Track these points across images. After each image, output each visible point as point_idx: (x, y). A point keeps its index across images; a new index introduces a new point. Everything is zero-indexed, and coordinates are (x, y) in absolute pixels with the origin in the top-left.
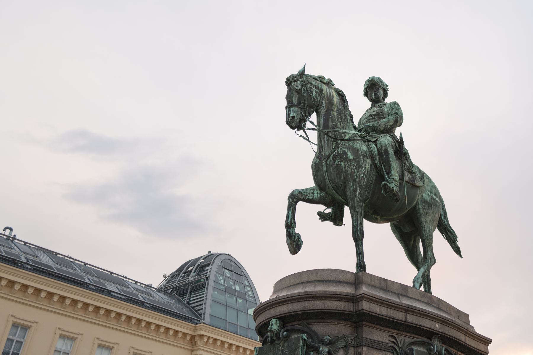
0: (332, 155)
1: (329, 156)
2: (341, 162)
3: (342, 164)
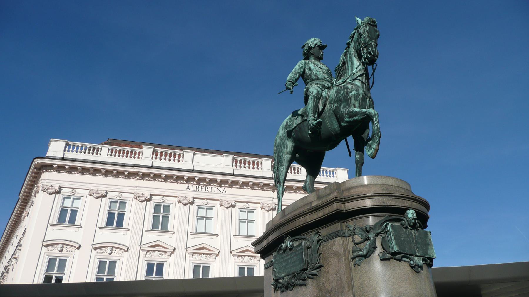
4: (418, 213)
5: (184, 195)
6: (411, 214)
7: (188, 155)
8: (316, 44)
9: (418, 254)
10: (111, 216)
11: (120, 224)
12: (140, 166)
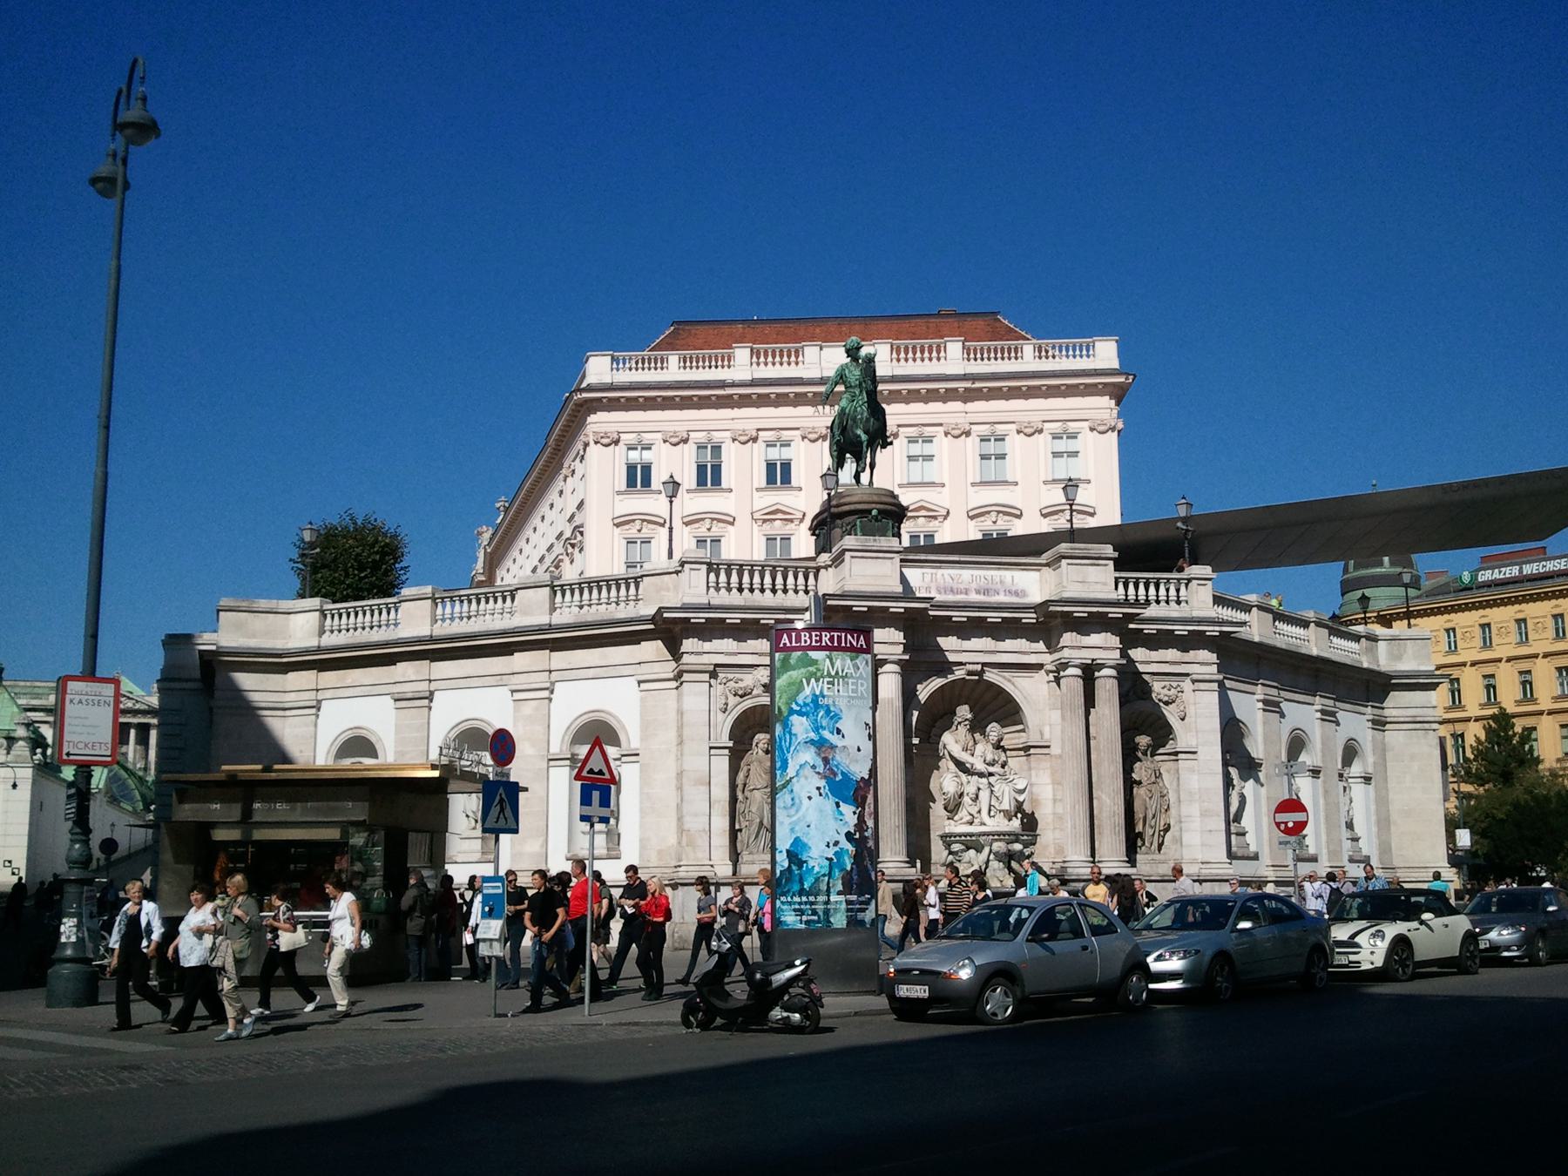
10: (701, 469)
11: (717, 481)
12: (733, 385)
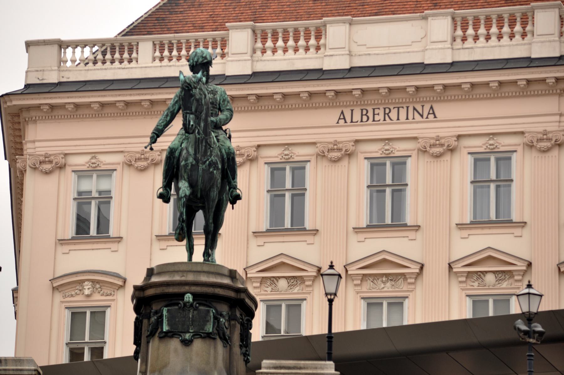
0: (208, 162)
1: (206, 161)
2: (214, 170)
3: (215, 172)
4: (195, 295)
5: (330, 138)
6: (189, 298)
7: (337, 32)
8: (196, 62)
9: (191, 331)
